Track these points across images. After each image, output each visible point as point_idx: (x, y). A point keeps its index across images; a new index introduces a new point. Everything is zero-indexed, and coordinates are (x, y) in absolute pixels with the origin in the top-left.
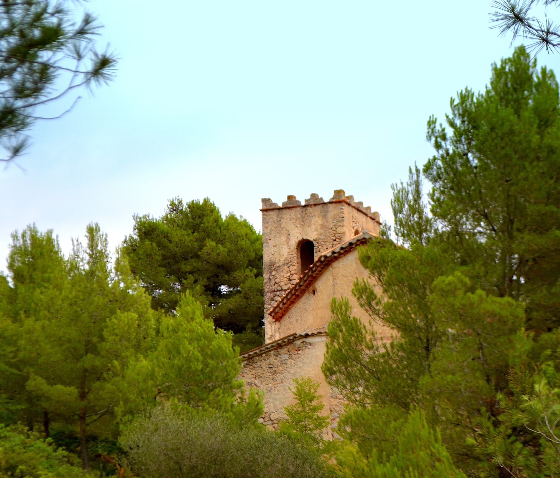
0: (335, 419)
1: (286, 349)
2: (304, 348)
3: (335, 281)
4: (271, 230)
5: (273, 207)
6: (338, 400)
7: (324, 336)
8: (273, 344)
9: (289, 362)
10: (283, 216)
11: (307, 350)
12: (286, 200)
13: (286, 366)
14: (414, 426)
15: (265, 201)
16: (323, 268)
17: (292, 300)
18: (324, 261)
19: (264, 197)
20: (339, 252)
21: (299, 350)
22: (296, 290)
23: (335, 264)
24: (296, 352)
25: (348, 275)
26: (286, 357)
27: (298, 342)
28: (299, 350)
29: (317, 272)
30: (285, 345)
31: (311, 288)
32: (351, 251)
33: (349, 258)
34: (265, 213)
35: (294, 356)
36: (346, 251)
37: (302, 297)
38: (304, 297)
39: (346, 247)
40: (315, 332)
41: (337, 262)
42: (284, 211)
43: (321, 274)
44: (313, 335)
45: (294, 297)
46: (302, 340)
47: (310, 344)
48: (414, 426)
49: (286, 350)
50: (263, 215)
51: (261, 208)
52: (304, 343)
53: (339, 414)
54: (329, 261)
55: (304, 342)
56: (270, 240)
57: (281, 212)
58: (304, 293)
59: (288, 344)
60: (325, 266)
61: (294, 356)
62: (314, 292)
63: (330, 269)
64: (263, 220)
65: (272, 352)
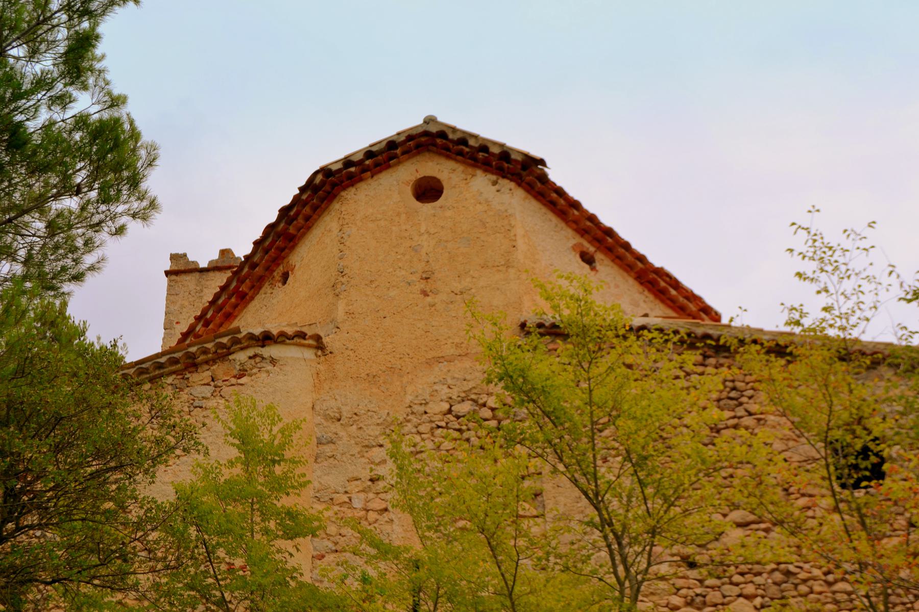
0: (323, 556)
1: (209, 373)
2: (255, 371)
3: (345, 229)
4: (182, 306)
5: (193, 267)
6: (336, 508)
7: (309, 346)
8: (176, 355)
9: (212, 403)
10: (208, 283)
11: (264, 375)
12: (216, 256)
13: (205, 413)
14: (865, 429)
15: (174, 257)
16: (315, 208)
17: (227, 308)
18: (323, 183)
19: (174, 252)
20: (360, 162)
21: (243, 375)
22: (241, 281)
23: (349, 194)
24: (233, 381)
25: (379, 216)
26: (208, 391)
27: (241, 357)
28: (240, 377)
29: (300, 220)
30: (207, 362)
31: (278, 273)
32: (389, 167)
33: (382, 181)
34: (173, 277)
35: (226, 391)
36: (377, 165)
37: (252, 298)
38: (258, 298)
39: (380, 152)
40: (290, 331)
41: (352, 190)
42: (211, 274)
43: (309, 228)
44: (282, 338)
45: (233, 300)
46: (251, 352)
47: (273, 361)
48: (865, 429)
49: (204, 375)
50: (170, 281)
51: (168, 268)
52: (258, 360)
53: (336, 544)
54: (334, 185)
55: (255, 356)
56: (177, 323)
57: (205, 276)
58: (260, 288)
59: (214, 361)
60: (322, 200)
61: (226, 391)
62: (285, 278)
63: (336, 205)
64: (168, 290)
65: (170, 380)
